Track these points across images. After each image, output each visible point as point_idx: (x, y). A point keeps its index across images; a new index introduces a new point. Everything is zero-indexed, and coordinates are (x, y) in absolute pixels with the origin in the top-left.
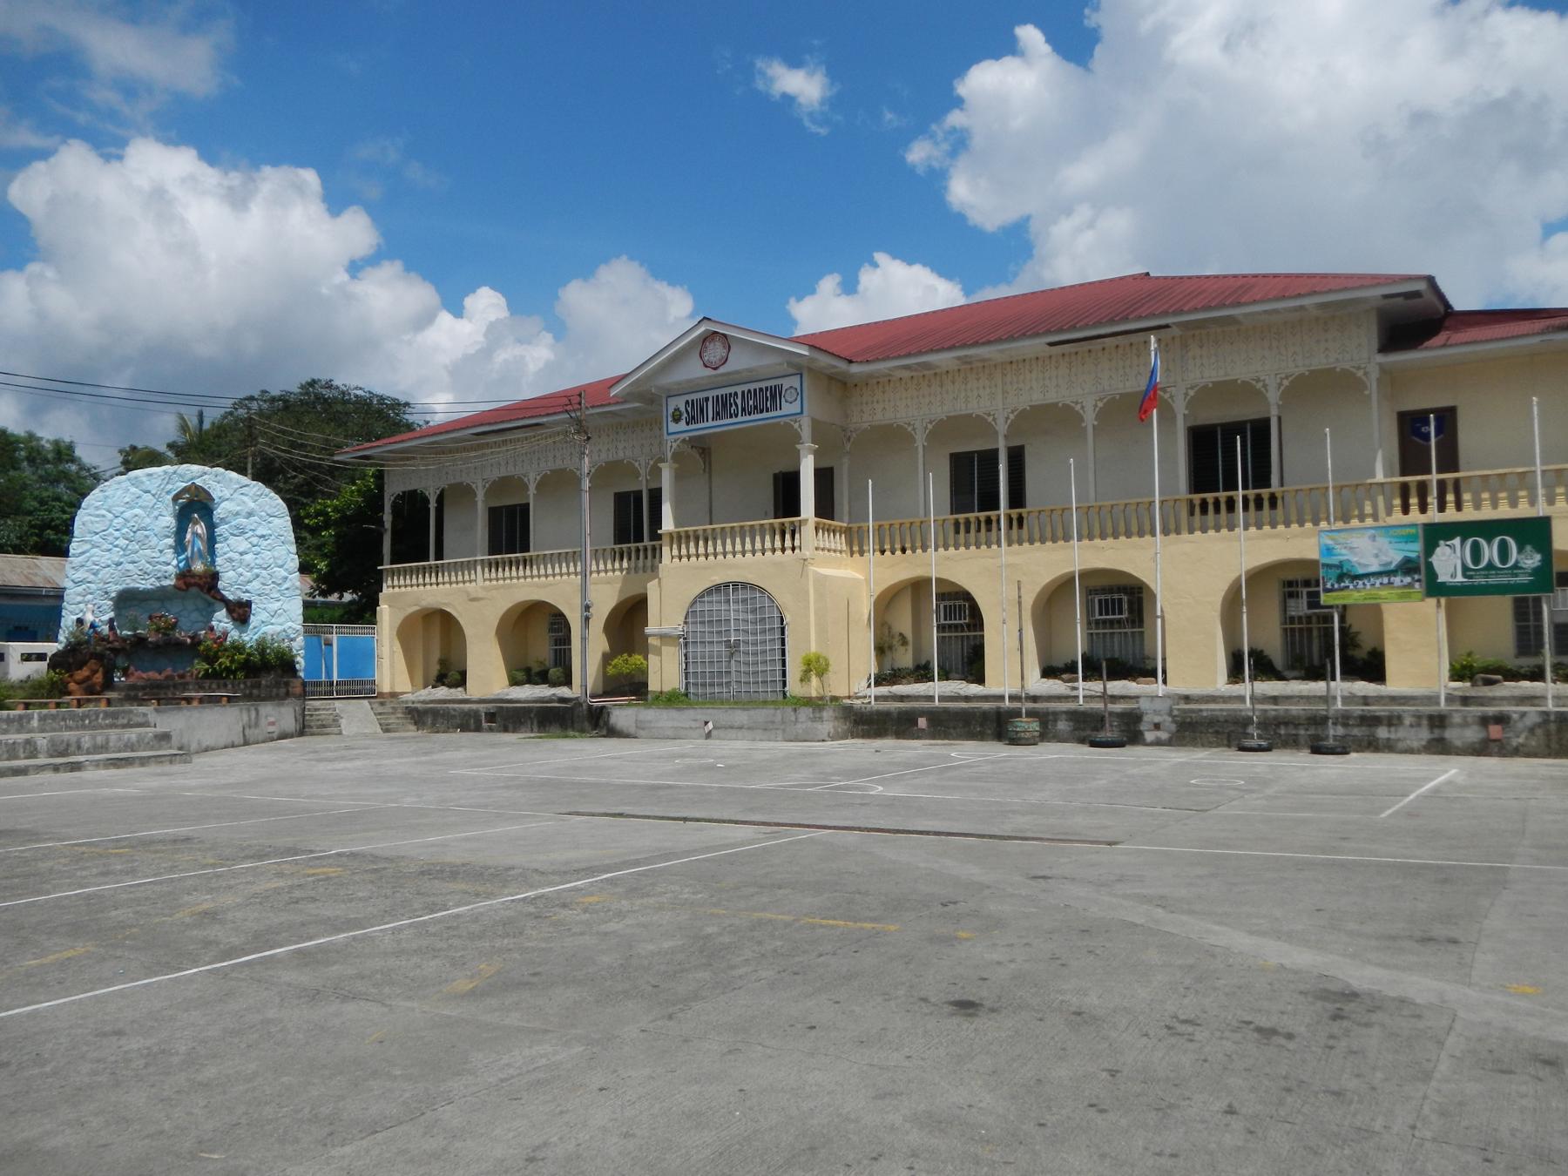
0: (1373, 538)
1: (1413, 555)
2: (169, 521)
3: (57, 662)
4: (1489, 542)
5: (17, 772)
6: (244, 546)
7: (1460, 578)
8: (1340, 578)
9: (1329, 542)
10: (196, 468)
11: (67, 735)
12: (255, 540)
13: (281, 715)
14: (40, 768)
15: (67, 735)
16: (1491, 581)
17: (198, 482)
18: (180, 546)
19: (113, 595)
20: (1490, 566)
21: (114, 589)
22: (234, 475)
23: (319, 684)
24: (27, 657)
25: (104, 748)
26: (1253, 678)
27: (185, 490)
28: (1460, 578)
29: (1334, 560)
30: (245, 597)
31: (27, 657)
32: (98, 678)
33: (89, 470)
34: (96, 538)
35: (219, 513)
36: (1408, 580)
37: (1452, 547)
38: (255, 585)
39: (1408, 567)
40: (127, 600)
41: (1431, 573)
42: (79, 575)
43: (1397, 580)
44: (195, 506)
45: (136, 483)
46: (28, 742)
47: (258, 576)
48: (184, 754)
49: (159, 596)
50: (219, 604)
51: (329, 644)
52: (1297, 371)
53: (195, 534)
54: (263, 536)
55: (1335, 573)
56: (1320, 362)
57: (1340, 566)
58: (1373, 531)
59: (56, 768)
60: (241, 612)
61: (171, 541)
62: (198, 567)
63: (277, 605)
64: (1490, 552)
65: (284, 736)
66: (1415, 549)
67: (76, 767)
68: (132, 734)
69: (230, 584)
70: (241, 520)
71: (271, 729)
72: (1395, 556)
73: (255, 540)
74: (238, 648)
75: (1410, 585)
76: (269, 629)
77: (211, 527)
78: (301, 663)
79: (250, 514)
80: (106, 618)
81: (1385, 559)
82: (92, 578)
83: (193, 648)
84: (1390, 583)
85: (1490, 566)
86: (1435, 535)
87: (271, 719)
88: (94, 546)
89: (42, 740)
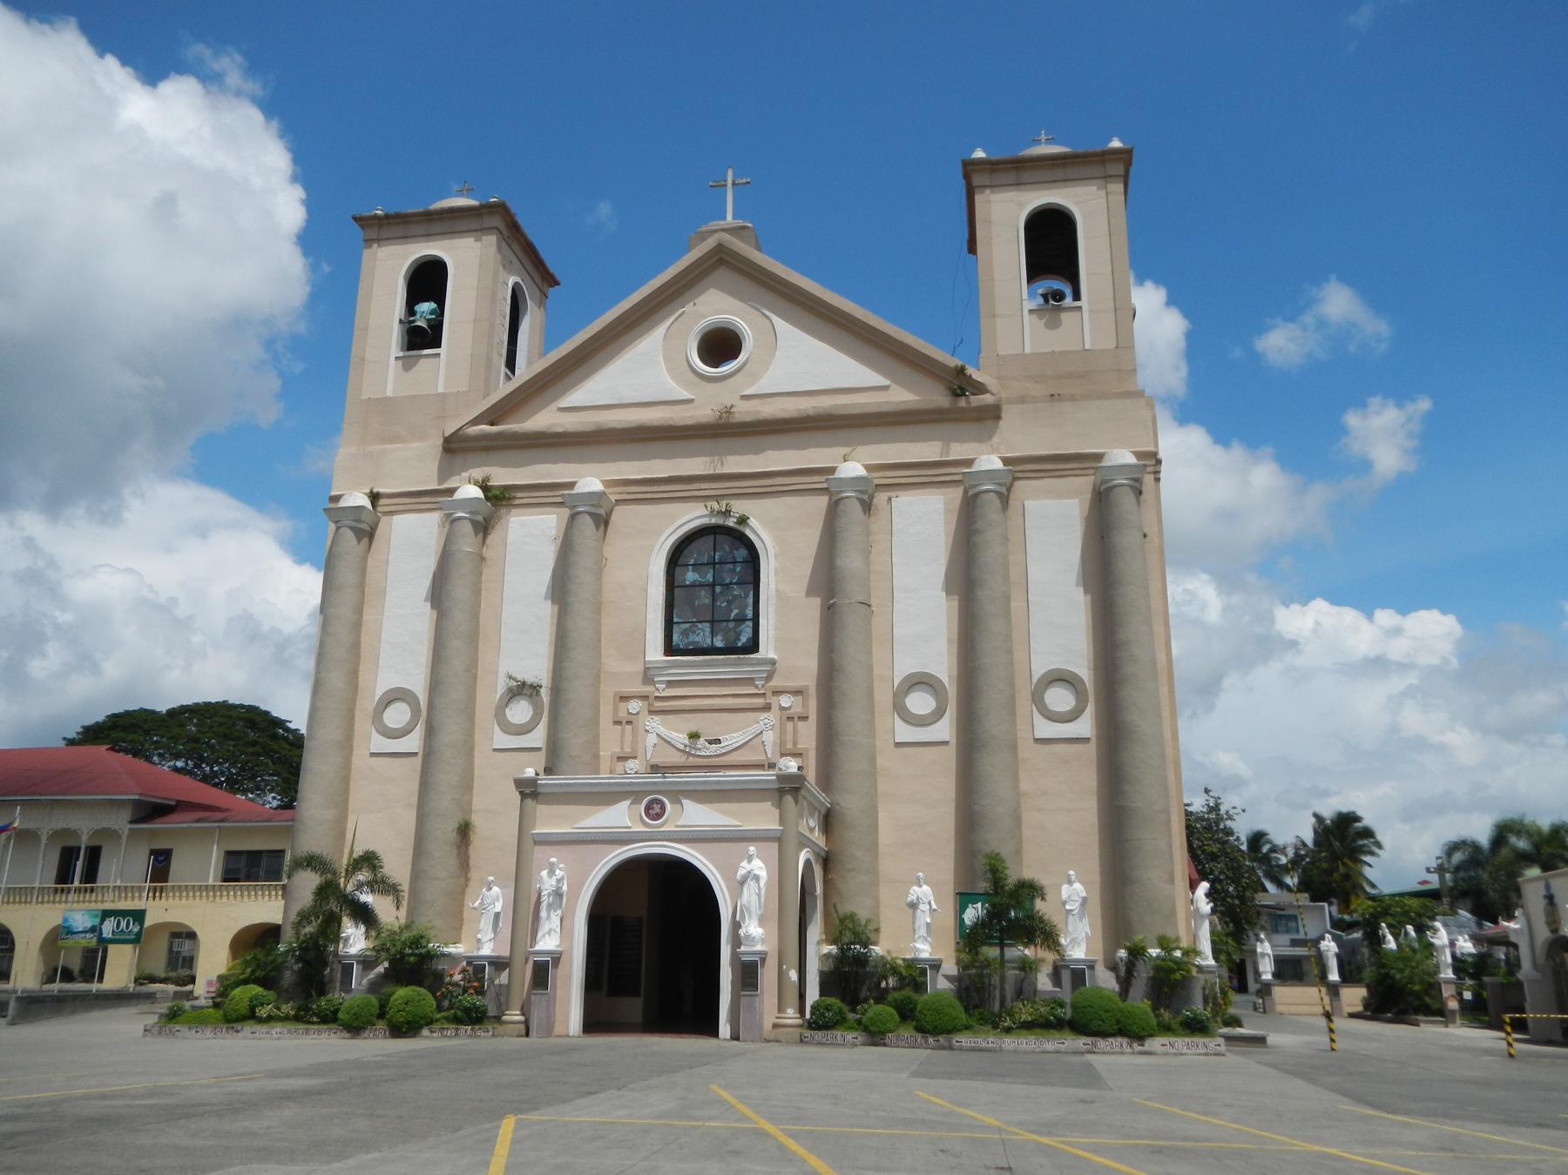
0: (83, 915)
1: (95, 924)
4: (124, 920)
7: (110, 936)
8: (67, 934)
9: (67, 916)
16: (123, 937)
20: (122, 930)
26: (61, 981)
28: (110, 936)
29: (67, 925)
36: (92, 935)
37: (110, 921)
39: (93, 930)
41: (101, 933)
43: (88, 935)
52: (96, 828)
55: (66, 930)
56: (105, 825)
57: (68, 928)
58: (83, 912)
64: (123, 924)
66: (97, 921)
72: (89, 925)
75: (92, 938)
81: (85, 925)
84: (85, 937)
85: (122, 930)
86: (106, 914)
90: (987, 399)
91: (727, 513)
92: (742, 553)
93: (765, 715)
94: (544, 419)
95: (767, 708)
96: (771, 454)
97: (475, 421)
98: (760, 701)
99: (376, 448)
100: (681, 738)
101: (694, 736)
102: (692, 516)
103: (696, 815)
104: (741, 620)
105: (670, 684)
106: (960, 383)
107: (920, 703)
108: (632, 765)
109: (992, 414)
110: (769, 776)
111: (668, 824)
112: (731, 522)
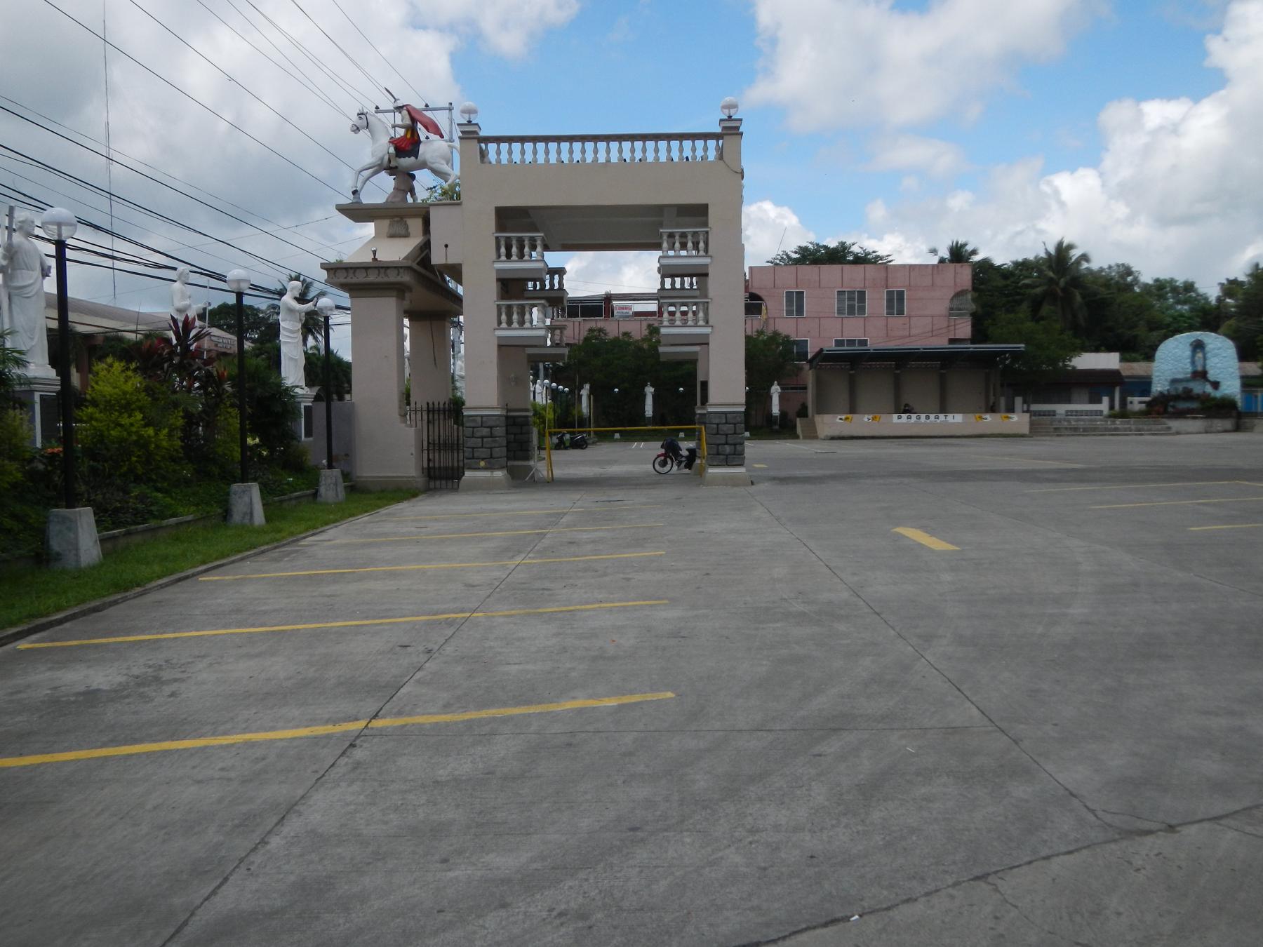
2: (1188, 353)
3: (1148, 404)
5: (1127, 435)
6: (1217, 361)
10: (1198, 333)
11: (1141, 426)
12: (1221, 358)
13: (1228, 424)
14: (1132, 434)
15: (1141, 426)
17: (1199, 338)
18: (1193, 363)
19: (1169, 380)
21: (1169, 378)
22: (1213, 334)
23: (1252, 413)
24: (1141, 402)
25: (1148, 430)
27: (1194, 341)
30: (1218, 380)
31: (1141, 402)
32: (1162, 410)
33: (1201, 296)
34: (1162, 361)
35: (1208, 348)
38: (1221, 375)
40: (1174, 381)
42: (1157, 374)
44: (1198, 346)
45: (1177, 340)
46: (1130, 428)
47: (1223, 372)
48: (1178, 433)
49: (1187, 380)
50: (1207, 383)
51: (1256, 397)
53: (1199, 357)
54: (1225, 357)
59: (1136, 435)
60: (1216, 385)
61: (1189, 360)
62: (1199, 368)
63: (1229, 383)
65: (1226, 431)
67: (1142, 435)
68: (1160, 427)
69: (1212, 375)
70: (1217, 351)
71: (1219, 428)
73: (1221, 358)
74: (1214, 399)
76: (1227, 392)
77: (1204, 355)
78: (1239, 404)
79: (1219, 349)
80: (1166, 388)
82: (1161, 374)
83: (1197, 398)
87: (1219, 425)
88: (1163, 363)
89: (1133, 427)
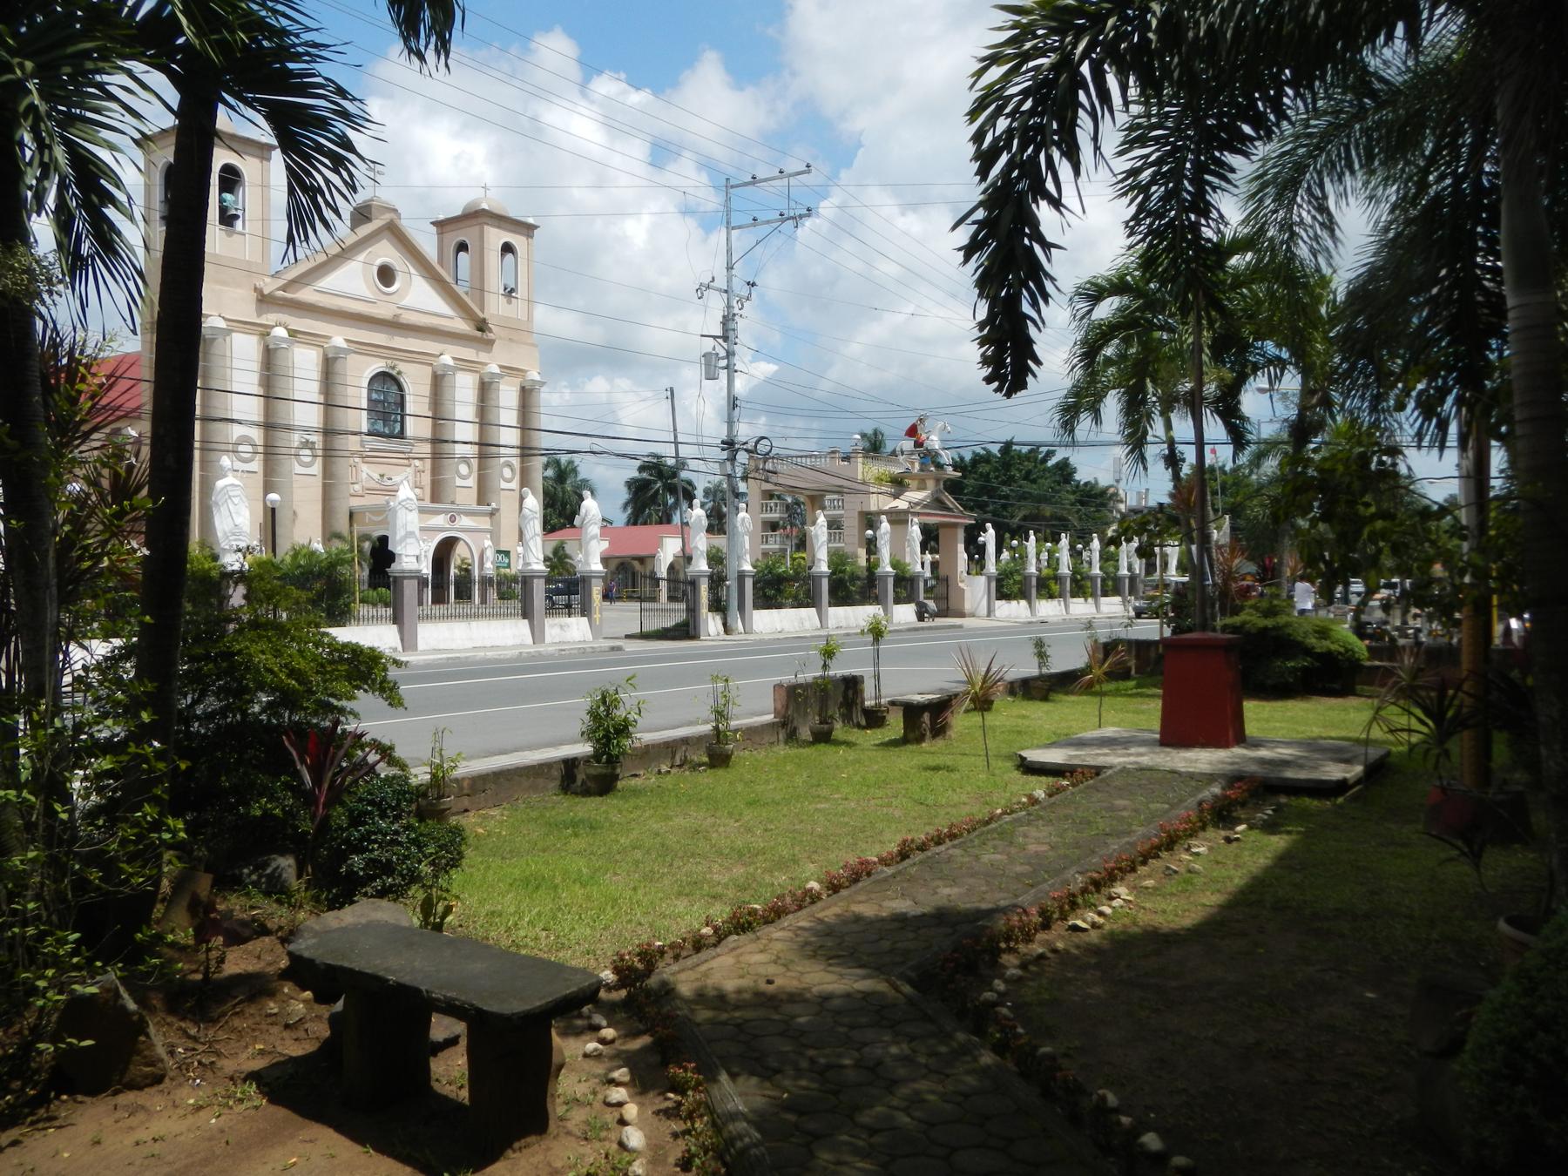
90: (491, 336)
91: (393, 368)
92: (394, 389)
93: (408, 469)
94: (306, 295)
95: (409, 466)
96: (411, 340)
97: (278, 289)
98: (406, 462)
99: (218, 287)
100: (376, 476)
101: (382, 476)
102: (378, 366)
103: (465, 521)
104: (396, 421)
105: (372, 450)
106: (482, 326)
107: (463, 469)
108: (356, 487)
109: (490, 343)
110: (489, 508)
111: (457, 524)
112: (394, 373)
